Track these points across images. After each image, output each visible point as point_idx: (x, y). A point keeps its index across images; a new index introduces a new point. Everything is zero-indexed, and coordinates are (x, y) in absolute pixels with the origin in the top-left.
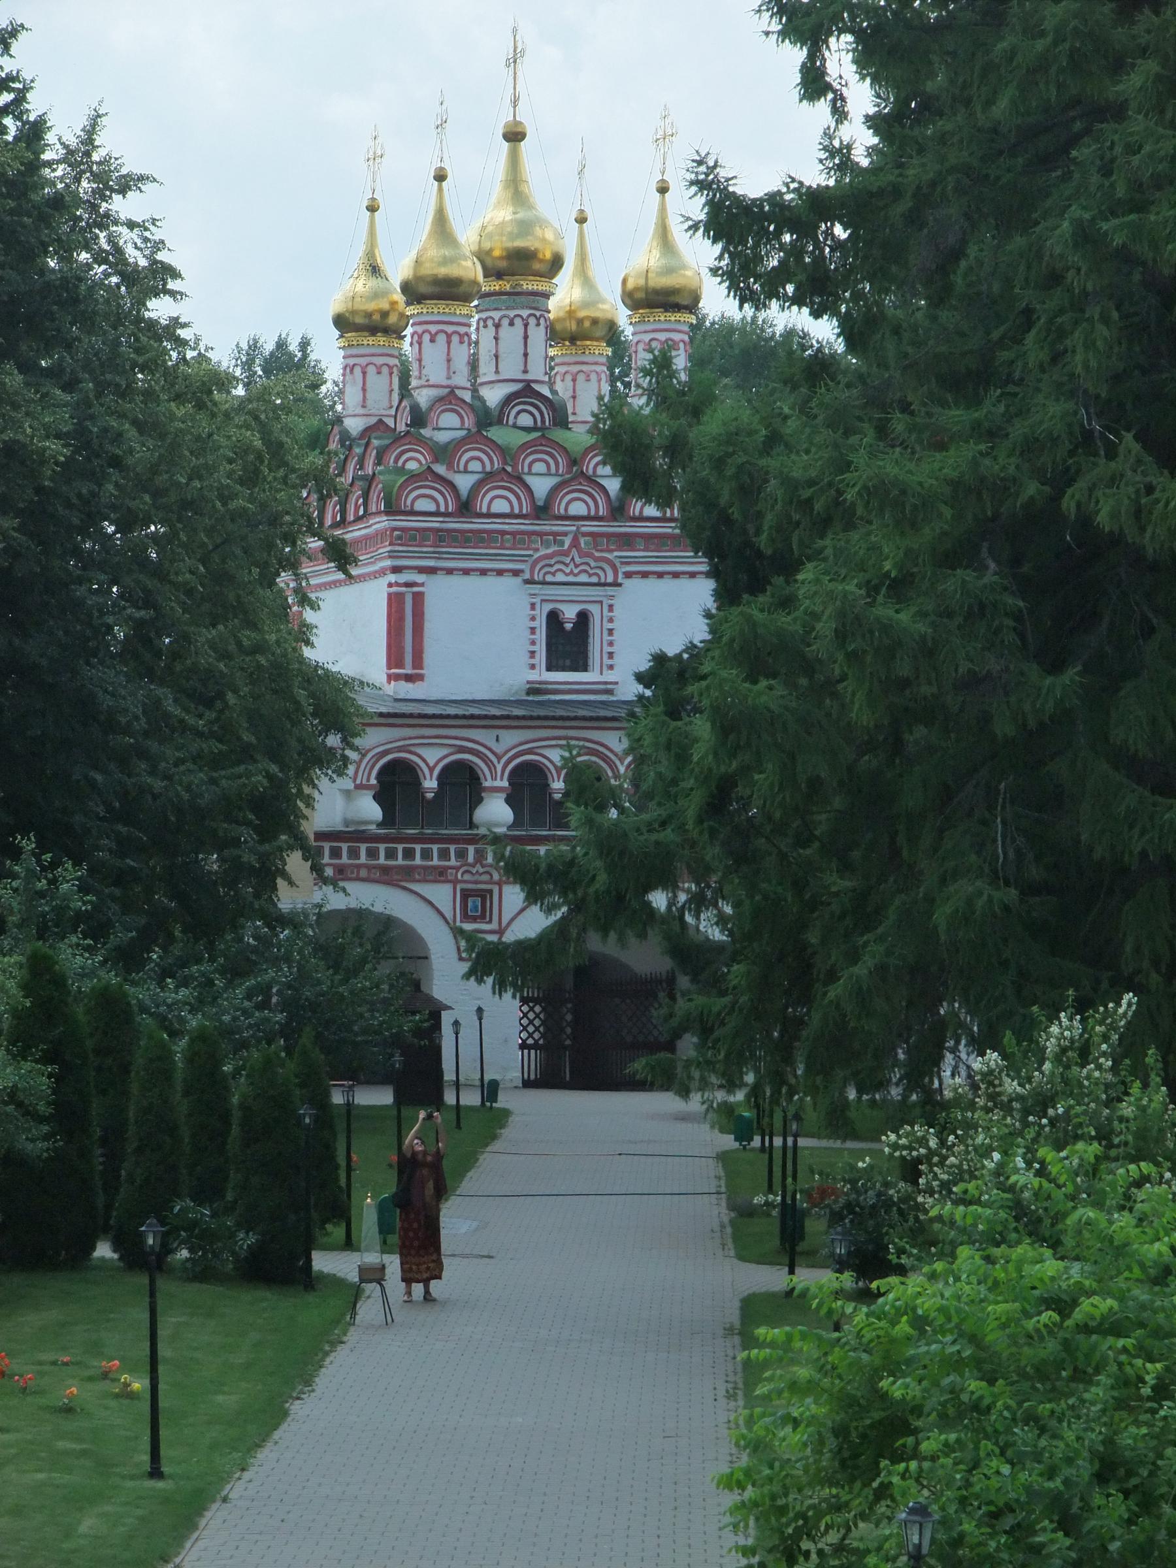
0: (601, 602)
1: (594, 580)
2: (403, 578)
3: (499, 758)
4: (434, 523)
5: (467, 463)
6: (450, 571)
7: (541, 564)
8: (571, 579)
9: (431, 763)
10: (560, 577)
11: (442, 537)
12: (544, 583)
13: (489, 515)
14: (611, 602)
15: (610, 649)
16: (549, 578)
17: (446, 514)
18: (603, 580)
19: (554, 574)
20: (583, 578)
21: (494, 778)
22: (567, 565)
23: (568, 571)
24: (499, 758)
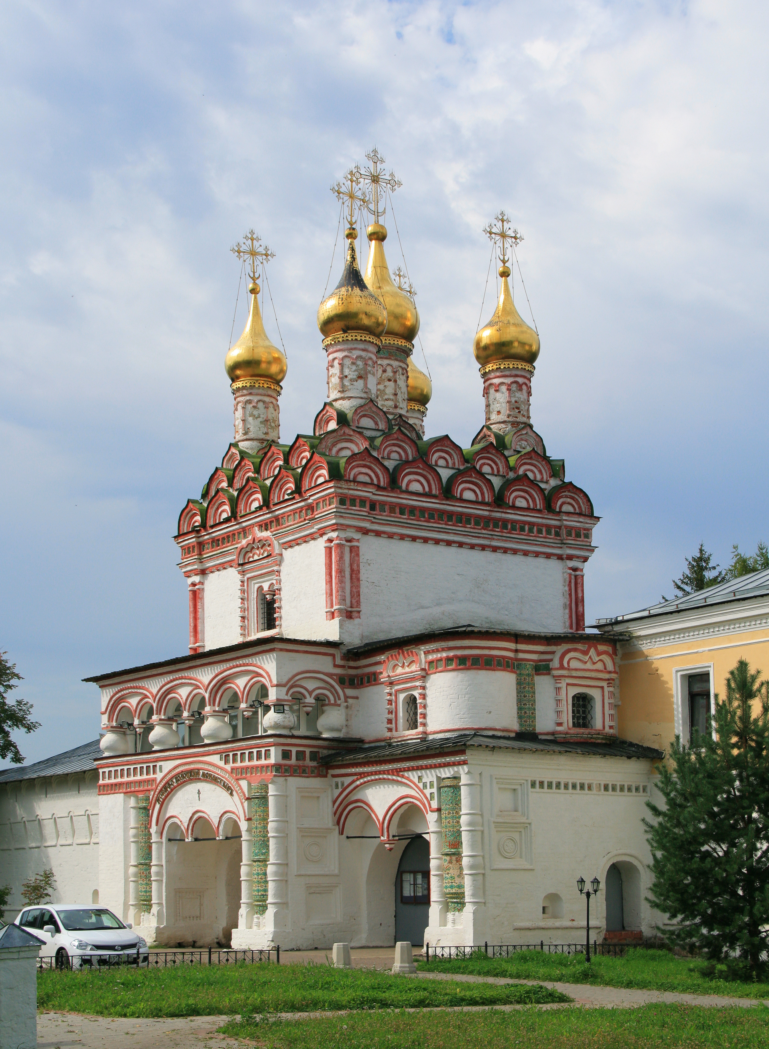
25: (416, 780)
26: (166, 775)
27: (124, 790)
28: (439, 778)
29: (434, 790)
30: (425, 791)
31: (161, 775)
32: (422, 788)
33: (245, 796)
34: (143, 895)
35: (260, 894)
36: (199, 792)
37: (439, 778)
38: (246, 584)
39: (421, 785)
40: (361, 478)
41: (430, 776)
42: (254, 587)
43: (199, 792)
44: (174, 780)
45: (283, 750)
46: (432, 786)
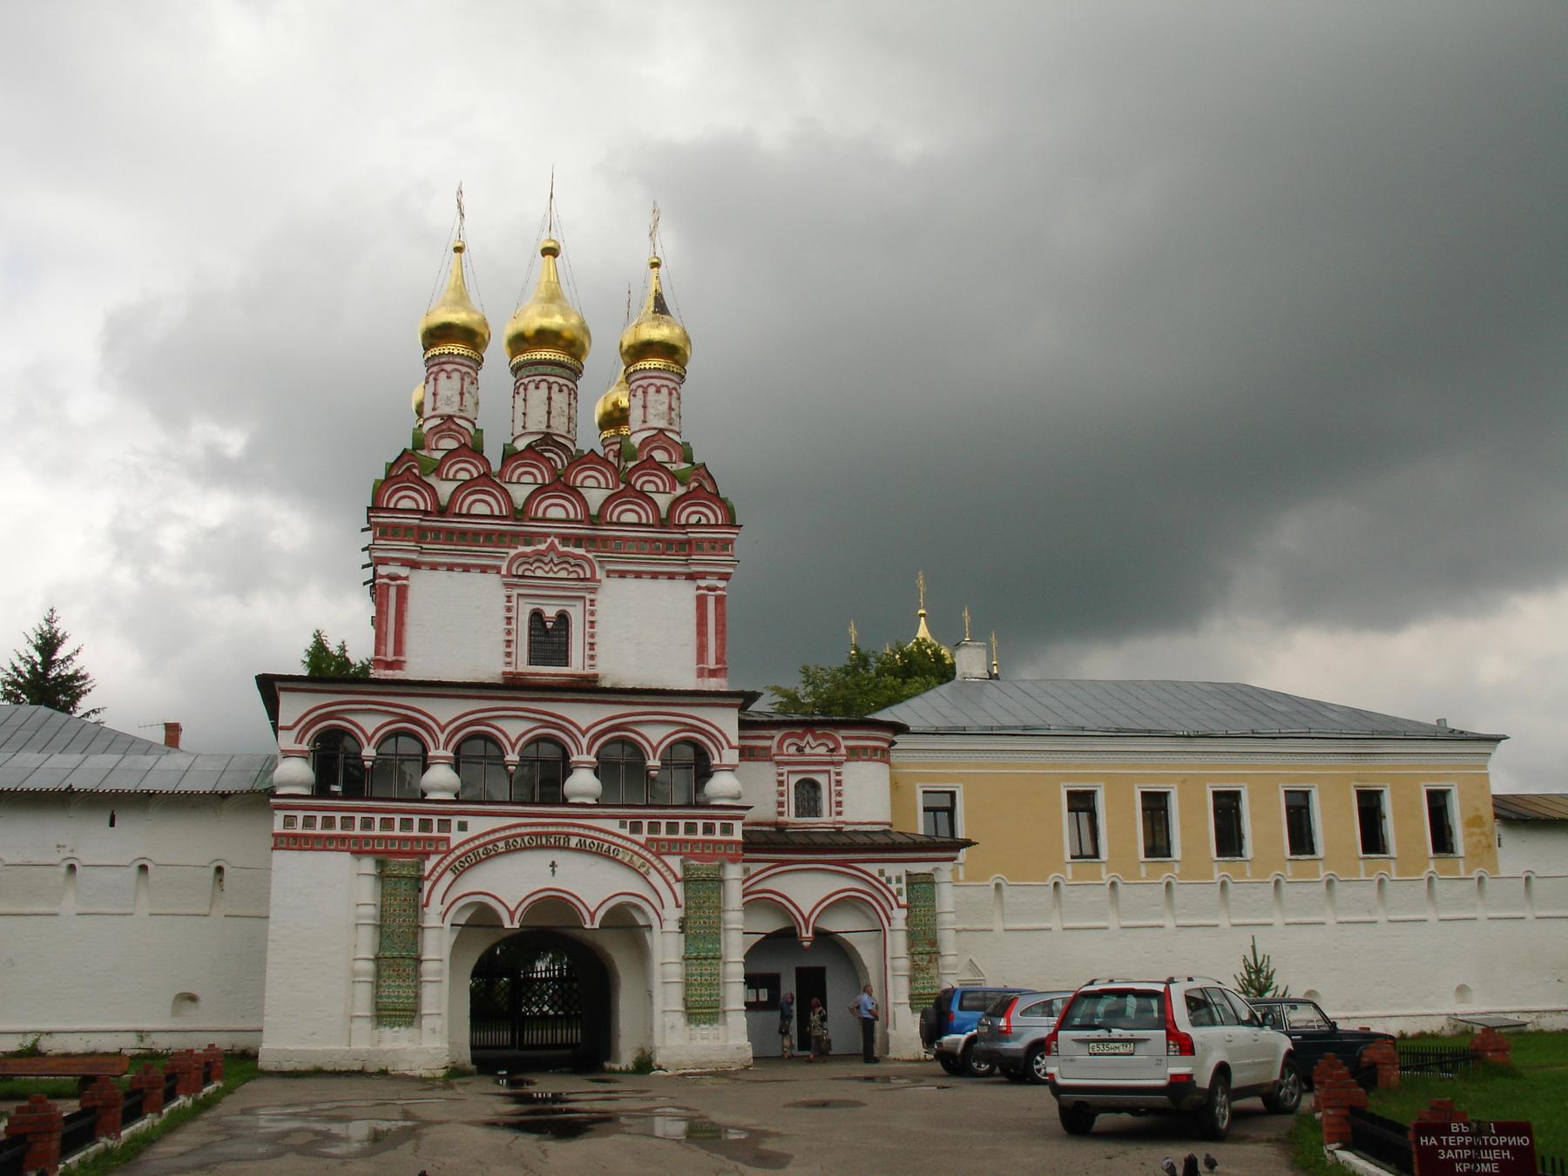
0: (583, 598)
1: (574, 576)
2: (382, 570)
3: (442, 729)
4: (413, 521)
5: (457, 472)
6: (434, 567)
7: (522, 560)
8: (551, 575)
9: (370, 732)
10: (539, 573)
11: (420, 534)
12: (523, 577)
13: (469, 515)
14: (592, 596)
15: (592, 641)
16: (527, 573)
17: (426, 512)
18: (582, 576)
19: (533, 572)
20: (563, 574)
21: (437, 748)
22: (546, 564)
23: (547, 569)
24: (442, 729)
25: (877, 875)
26: (473, 839)
27: (356, 848)
28: (909, 875)
29: (903, 886)
30: (889, 885)
31: (464, 836)
32: (885, 882)
33: (675, 875)
34: (412, 1003)
35: (703, 999)
36: (553, 865)
37: (909, 875)
38: (514, 603)
39: (883, 880)
40: (625, 518)
41: (893, 870)
42: (526, 609)
43: (553, 865)
44: (501, 844)
45: (704, 823)
46: (899, 880)
